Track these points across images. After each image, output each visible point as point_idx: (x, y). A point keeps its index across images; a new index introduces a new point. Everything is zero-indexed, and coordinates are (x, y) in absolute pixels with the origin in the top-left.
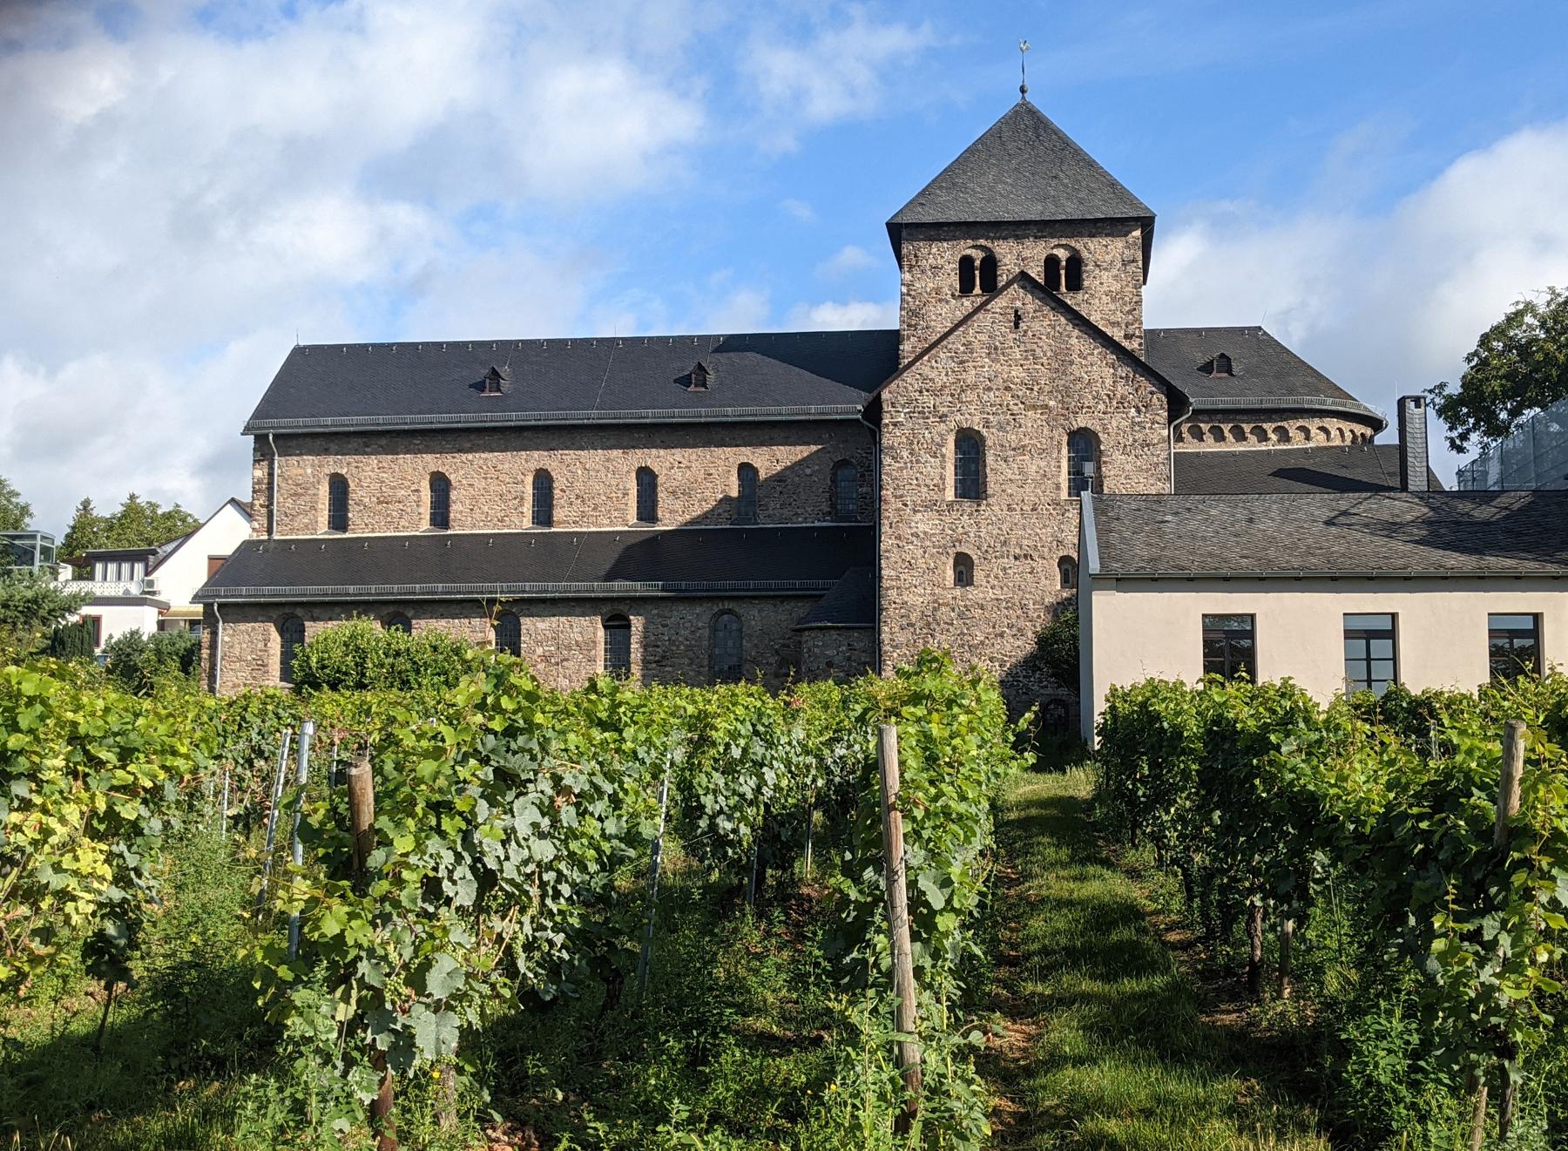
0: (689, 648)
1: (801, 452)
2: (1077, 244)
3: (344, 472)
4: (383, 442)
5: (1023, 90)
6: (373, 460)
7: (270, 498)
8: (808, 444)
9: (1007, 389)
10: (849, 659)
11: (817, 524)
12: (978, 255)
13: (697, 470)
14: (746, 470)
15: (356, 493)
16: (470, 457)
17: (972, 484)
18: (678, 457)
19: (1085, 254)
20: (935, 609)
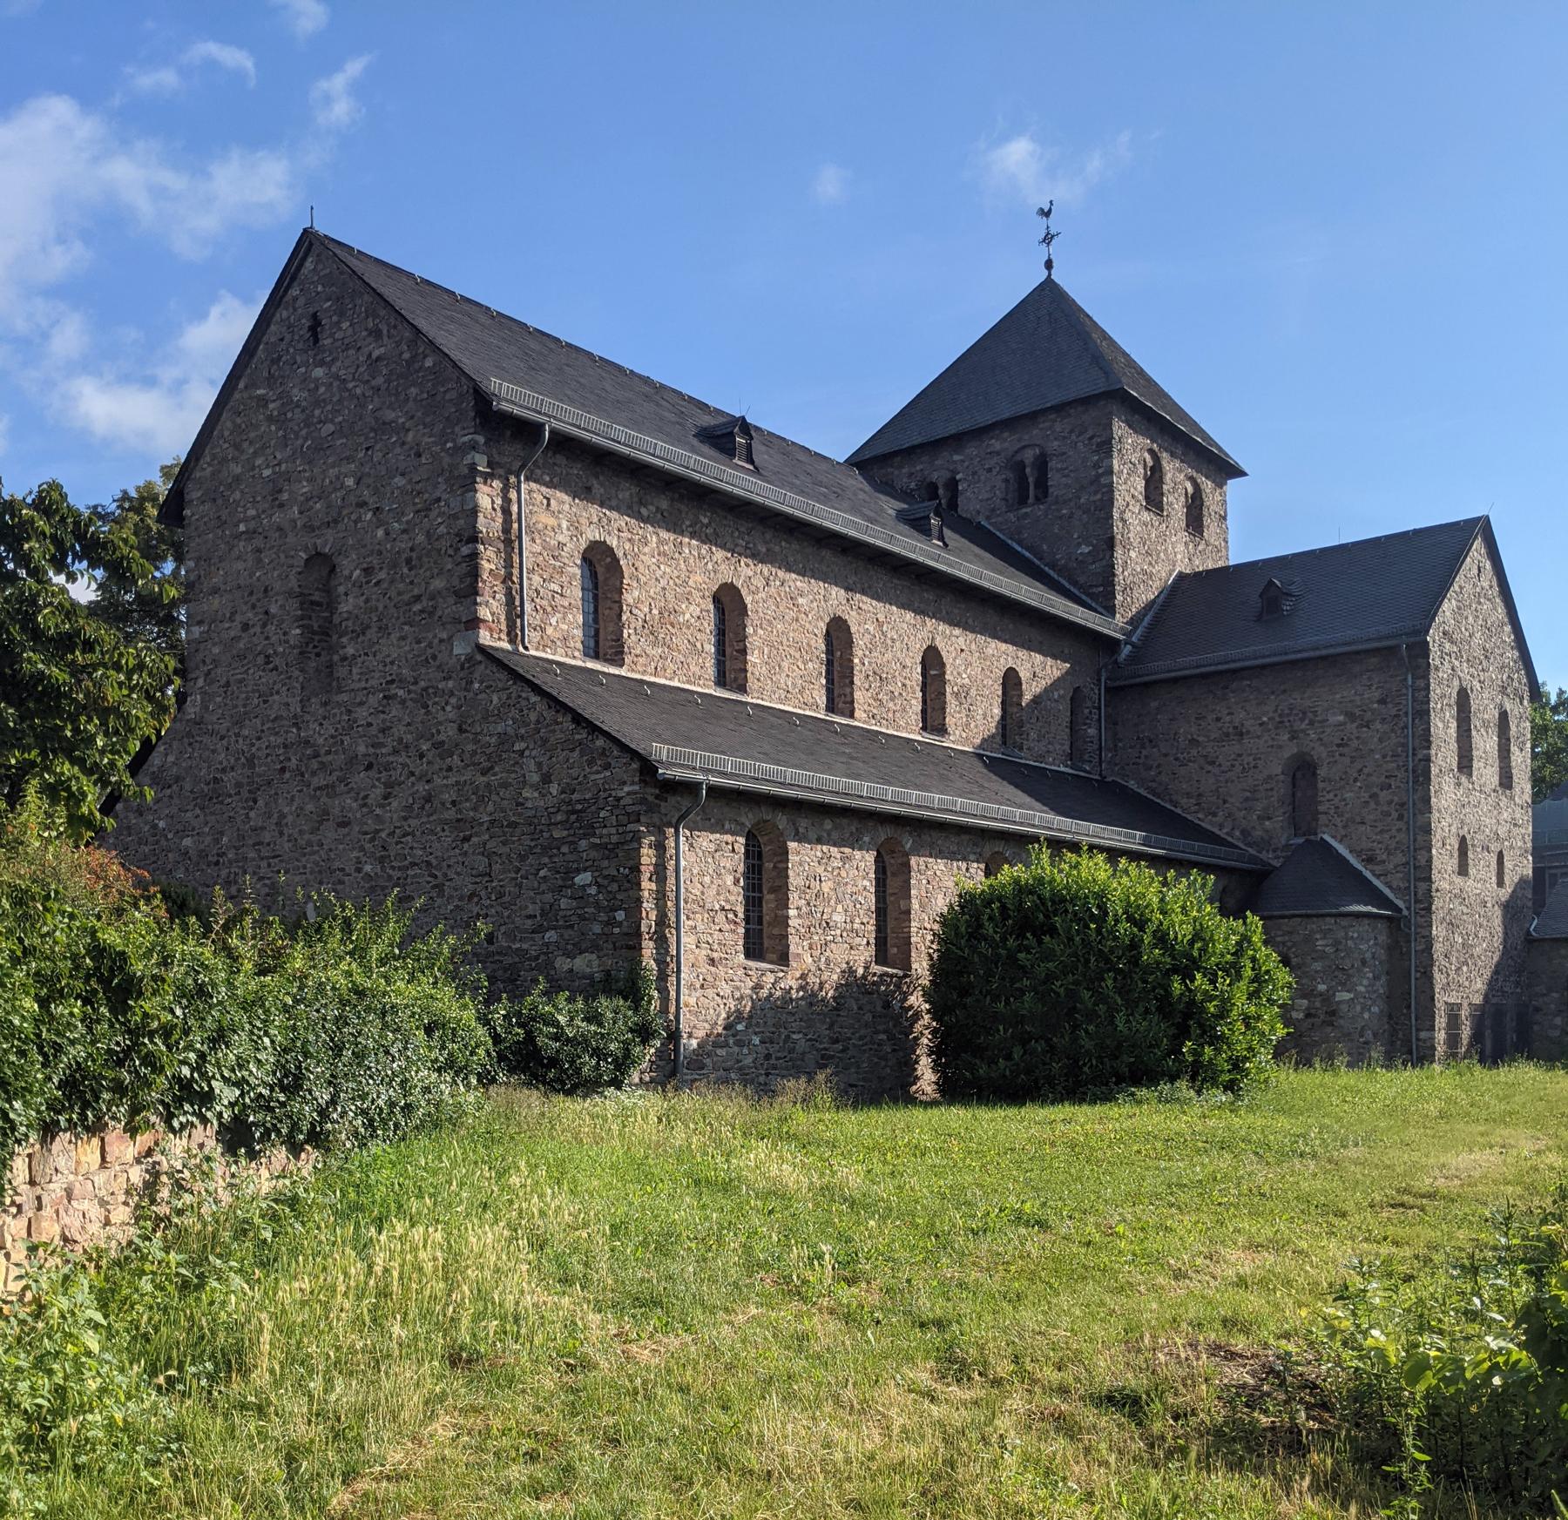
11: (1062, 769)
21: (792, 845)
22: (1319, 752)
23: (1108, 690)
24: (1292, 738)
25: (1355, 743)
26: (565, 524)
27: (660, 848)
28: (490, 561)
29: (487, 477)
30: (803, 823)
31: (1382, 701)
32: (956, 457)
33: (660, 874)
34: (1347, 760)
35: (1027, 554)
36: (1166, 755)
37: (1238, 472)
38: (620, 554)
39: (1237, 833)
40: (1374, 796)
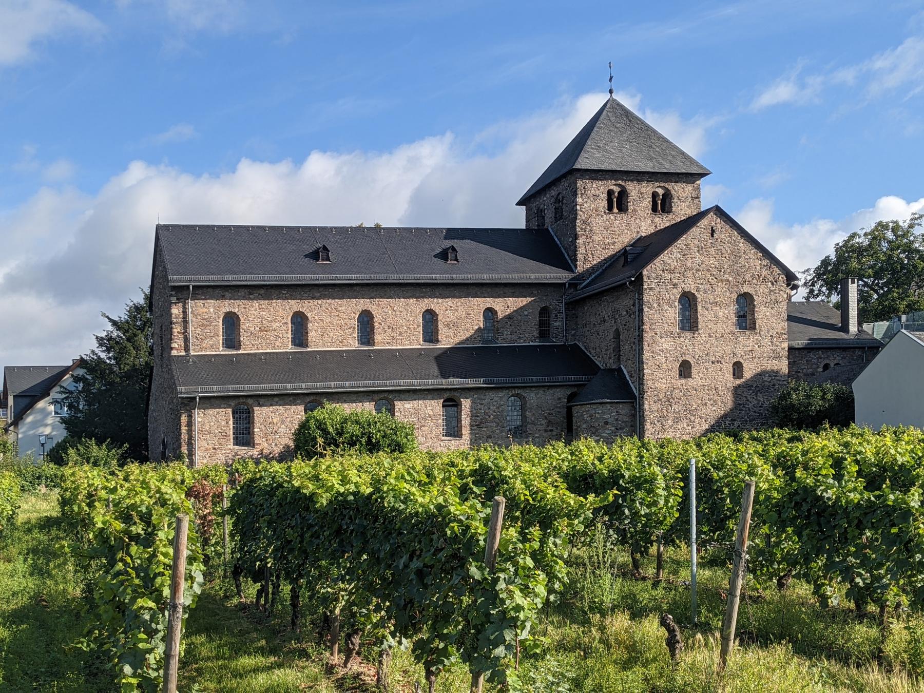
1: (522, 302)
2: (669, 186)
3: (236, 311)
4: (262, 292)
6: (256, 304)
7: (185, 327)
8: (525, 296)
12: (617, 189)
13: (462, 312)
14: (490, 313)
15: (245, 325)
16: (320, 302)
17: (689, 322)
18: (450, 303)
19: (673, 192)
20: (672, 391)
21: (255, 408)
22: (621, 329)
26: (212, 310)
27: (190, 417)
28: (177, 329)
29: (175, 303)
30: (262, 401)
33: (190, 424)
38: (239, 313)
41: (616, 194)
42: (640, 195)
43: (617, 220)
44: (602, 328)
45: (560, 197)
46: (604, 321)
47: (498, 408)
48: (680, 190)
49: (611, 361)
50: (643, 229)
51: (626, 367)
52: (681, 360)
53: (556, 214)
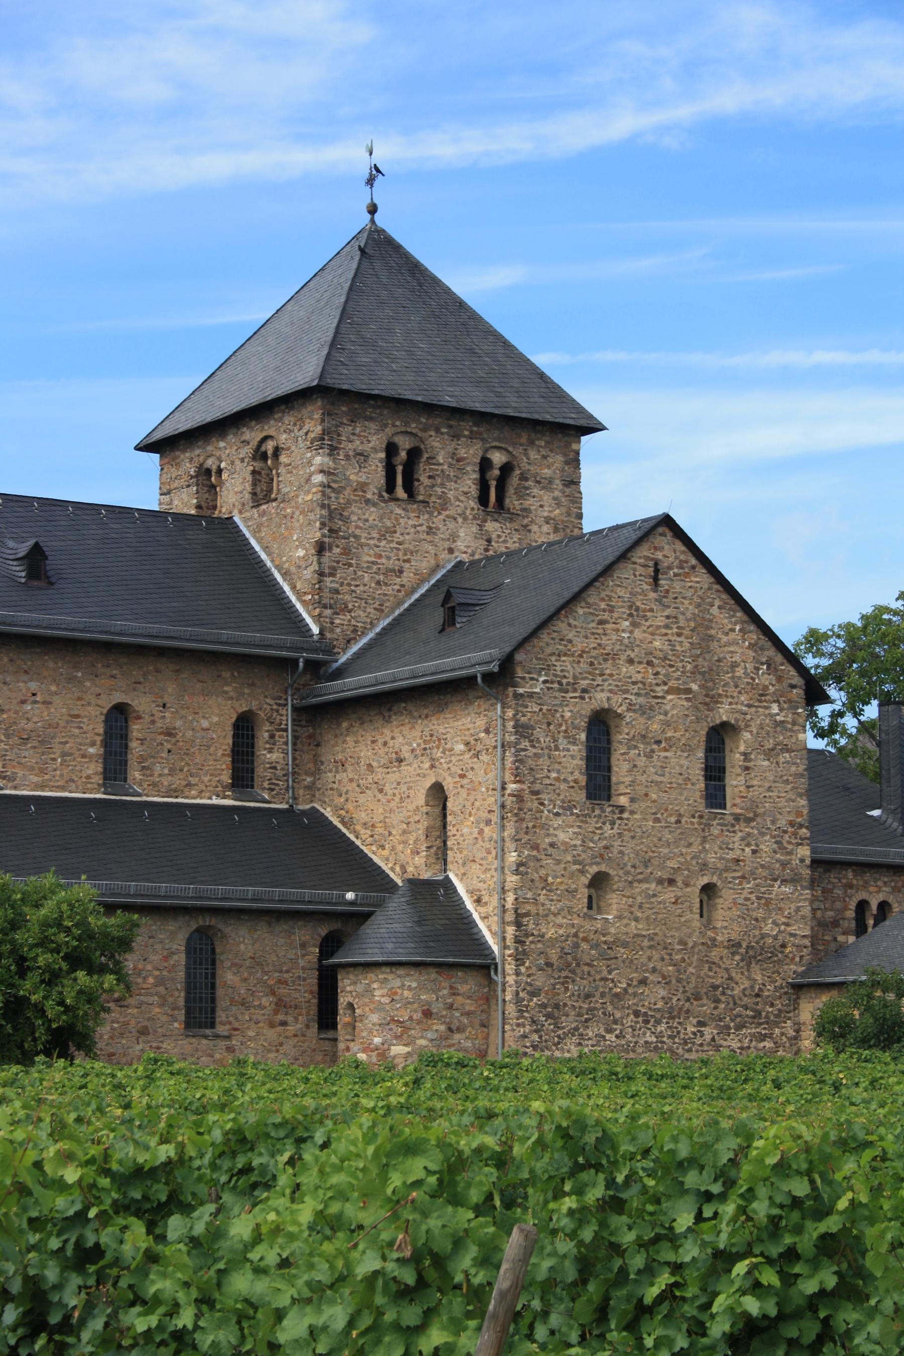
0: (160, 981)
5: (373, 209)
9: (650, 663)
10: (450, 1007)
11: (215, 801)
12: (405, 444)
22: (449, 784)
23: (295, 709)
24: (432, 767)
25: (470, 774)
31: (487, 731)
32: (222, 444)
34: (463, 793)
35: (263, 556)
36: (351, 780)
37: (594, 427)
39: (398, 869)
40: (481, 832)
41: (403, 454)
42: (455, 465)
43: (407, 520)
44: (394, 777)
45: (270, 446)
46: (400, 761)
47: (166, 958)
48: (539, 460)
49: (419, 860)
50: (460, 545)
51: (463, 876)
52: (594, 869)
53: (254, 484)
